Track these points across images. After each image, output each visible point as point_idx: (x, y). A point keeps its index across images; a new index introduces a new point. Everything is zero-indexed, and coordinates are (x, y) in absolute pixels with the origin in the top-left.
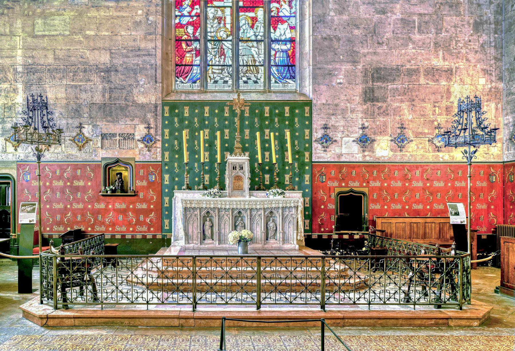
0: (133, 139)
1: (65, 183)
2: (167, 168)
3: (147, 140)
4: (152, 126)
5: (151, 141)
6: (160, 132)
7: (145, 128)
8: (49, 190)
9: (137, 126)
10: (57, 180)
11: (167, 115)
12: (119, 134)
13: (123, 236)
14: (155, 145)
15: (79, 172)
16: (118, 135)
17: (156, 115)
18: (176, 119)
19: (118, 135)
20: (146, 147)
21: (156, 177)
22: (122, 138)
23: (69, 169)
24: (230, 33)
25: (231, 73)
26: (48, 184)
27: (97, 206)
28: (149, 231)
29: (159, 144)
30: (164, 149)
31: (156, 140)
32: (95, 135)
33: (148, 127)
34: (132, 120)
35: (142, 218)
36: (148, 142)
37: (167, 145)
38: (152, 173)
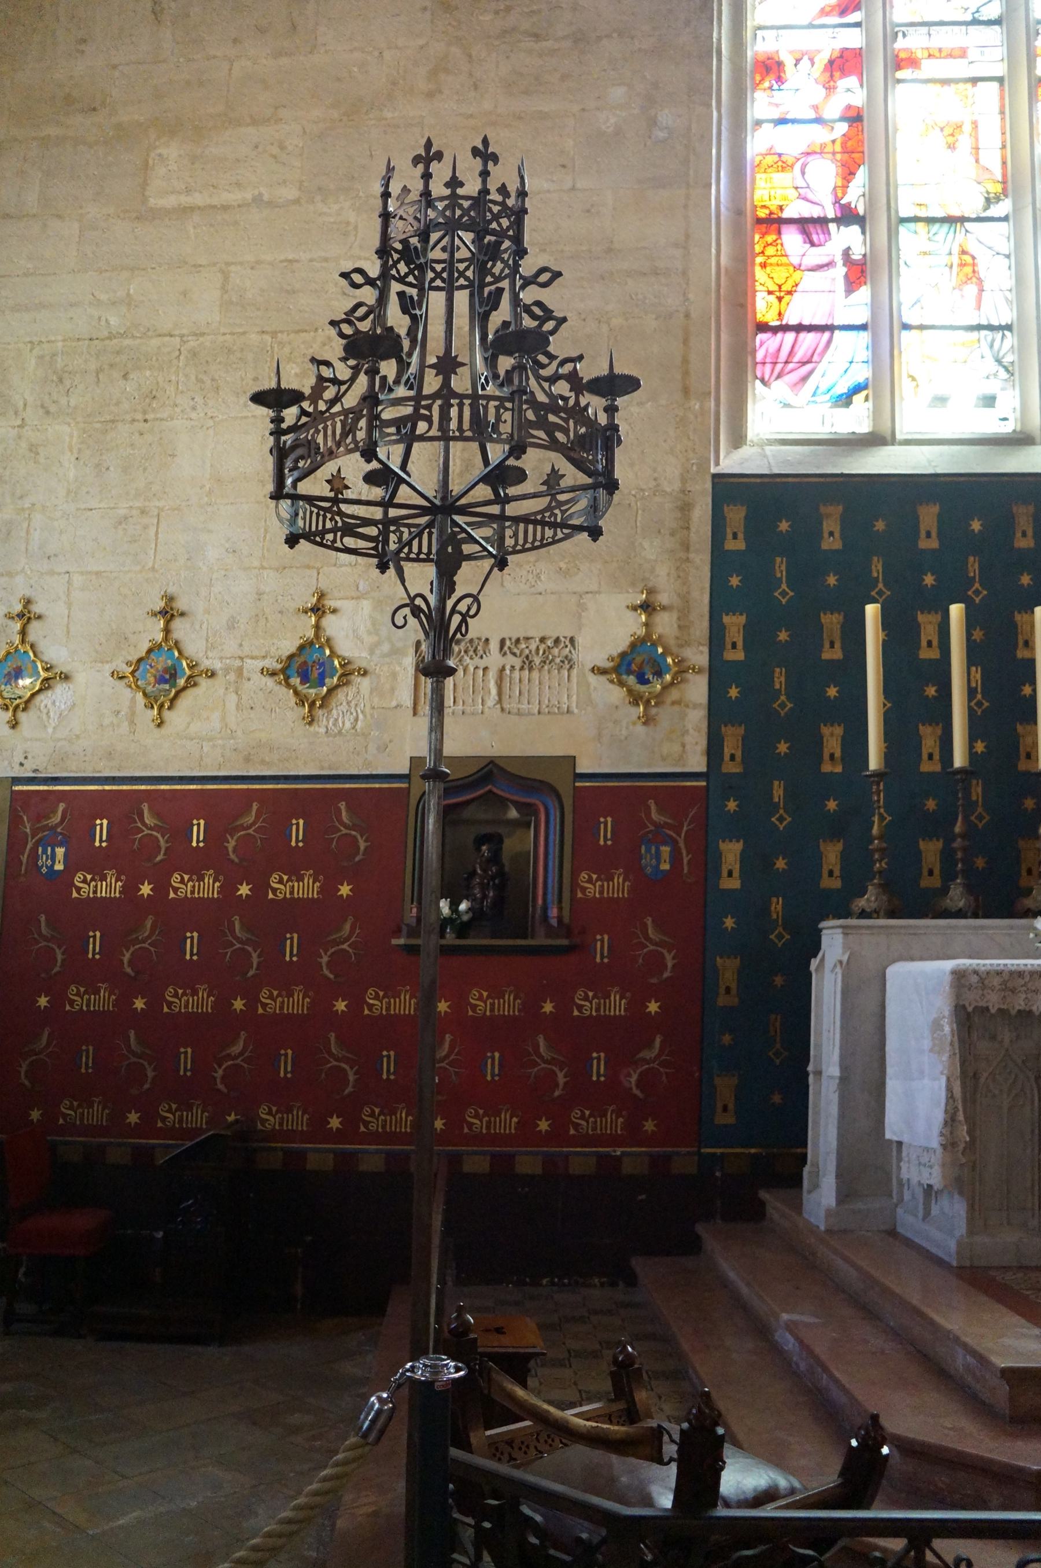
0: (569, 662)
1: (229, 888)
2: (732, 805)
3: (638, 667)
4: (663, 599)
5: (659, 674)
6: (701, 627)
7: (634, 608)
8: (149, 923)
9: (587, 599)
10: (191, 873)
11: (740, 545)
12: (503, 642)
13: (503, 1163)
14: (674, 694)
15: (298, 829)
16: (494, 646)
17: (686, 547)
18: (781, 567)
19: (494, 646)
20: (635, 699)
21: (676, 858)
22: (517, 662)
23: (250, 819)
24: (999, 188)
25: (1008, 359)
26: (146, 890)
27: (375, 1003)
28: (633, 1135)
29: (698, 689)
30: (718, 712)
31: (683, 669)
32: (386, 647)
33: (647, 607)
34: (565, 574)
35: (598, 1068)
36: (643, 680)
37: (734, 692)
38: (659, 837)
